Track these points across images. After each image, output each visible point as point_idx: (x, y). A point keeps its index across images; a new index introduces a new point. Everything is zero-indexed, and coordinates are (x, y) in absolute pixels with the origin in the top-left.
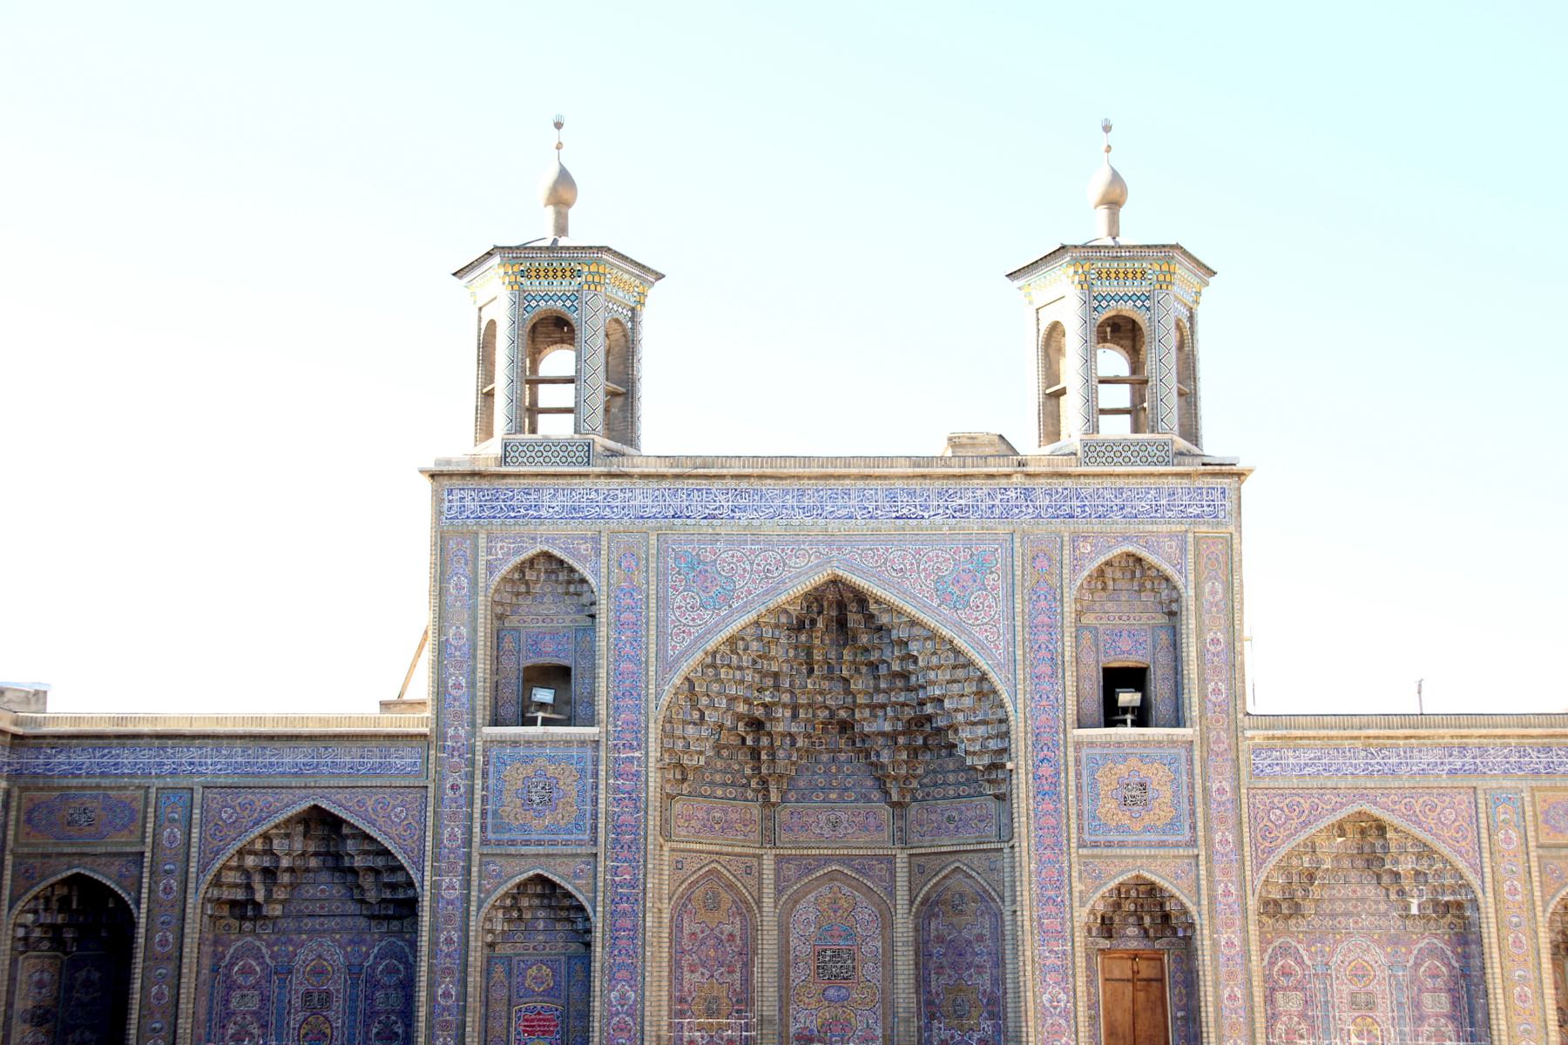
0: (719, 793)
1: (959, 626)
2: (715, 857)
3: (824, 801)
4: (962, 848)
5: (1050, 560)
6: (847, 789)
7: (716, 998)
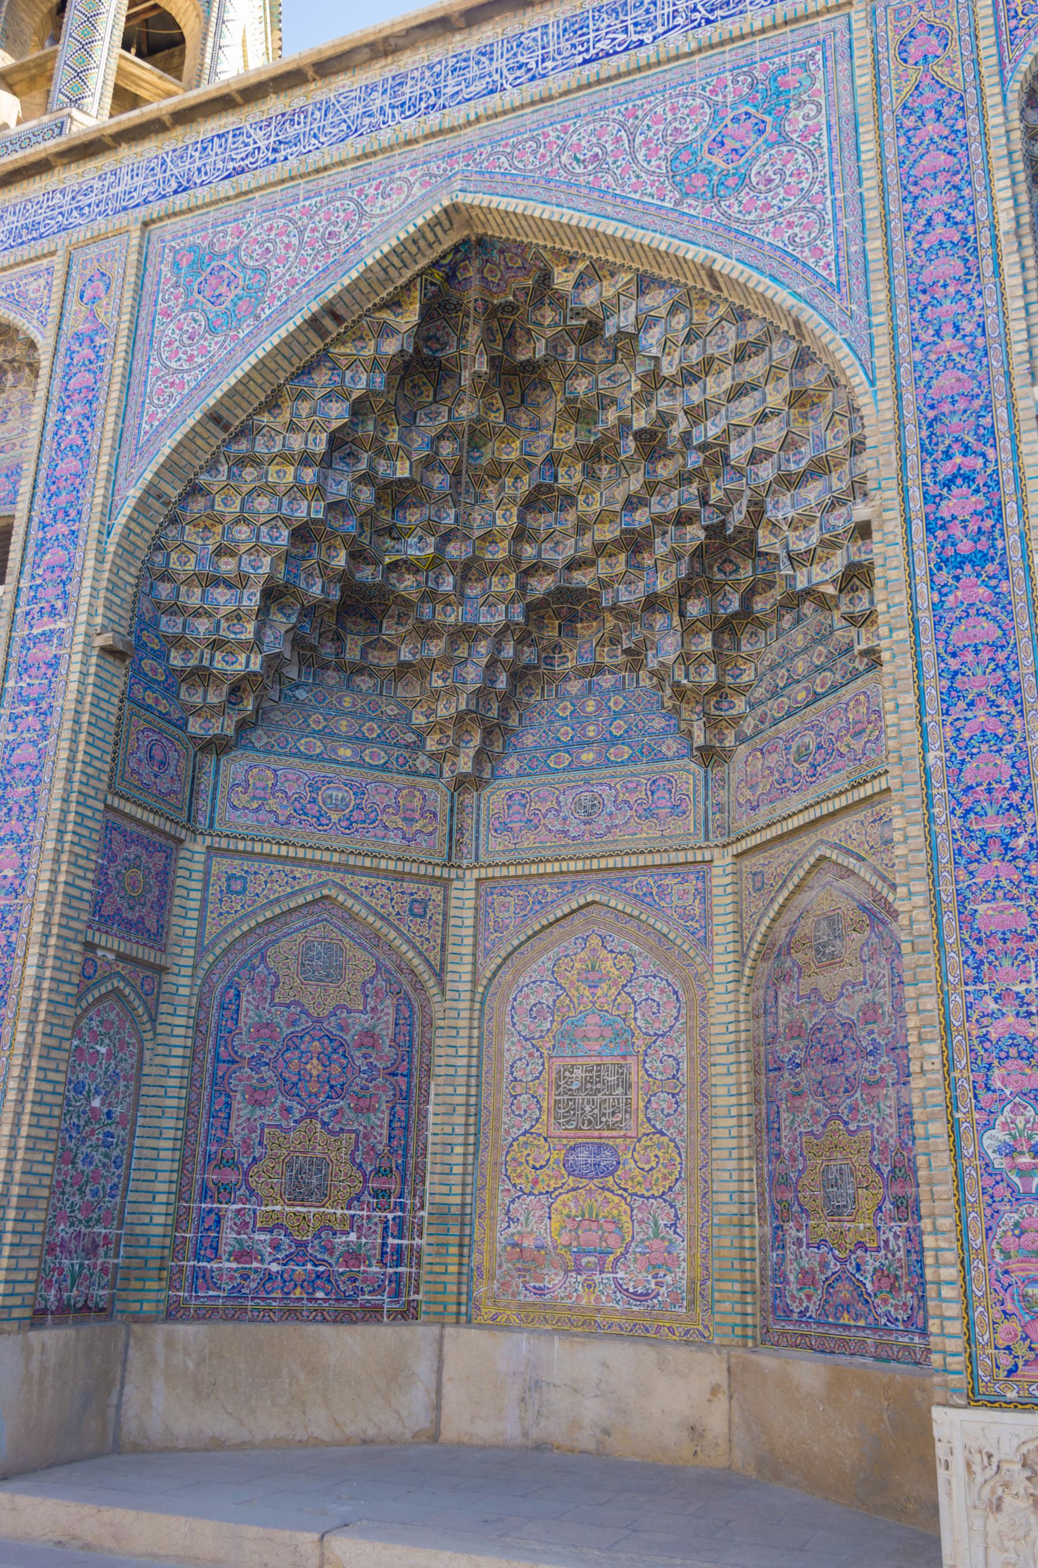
0: (345, 752)
1: (729, 232)
2: (337, 877)
3: (569, 768)
4: (827, 808)
5: (943, 36)
6: (614, 741)
7: (320, 1165)
